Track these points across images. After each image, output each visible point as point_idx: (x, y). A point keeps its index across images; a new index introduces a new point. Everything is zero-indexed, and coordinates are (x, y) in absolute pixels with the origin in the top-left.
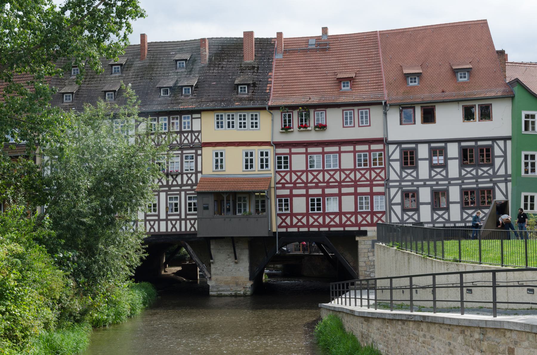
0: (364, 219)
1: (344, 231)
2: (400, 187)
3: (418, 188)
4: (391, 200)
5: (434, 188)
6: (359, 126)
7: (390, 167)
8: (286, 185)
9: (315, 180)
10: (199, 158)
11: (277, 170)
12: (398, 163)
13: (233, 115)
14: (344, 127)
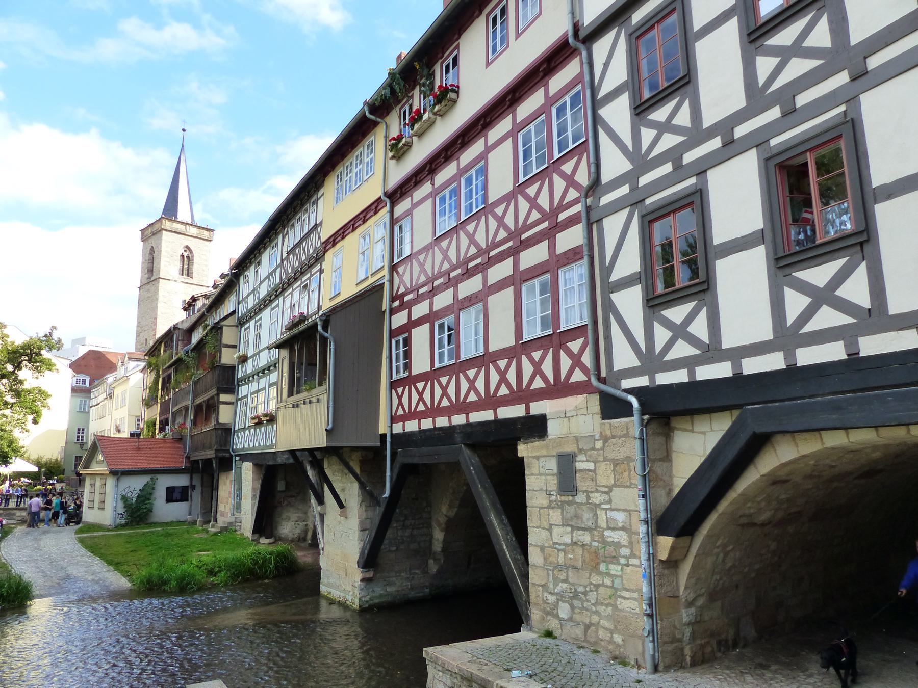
0: (538, 370)
1: (497, 422)
2: (634, 202)
3: (702, 173)
4: (607, 270)
5: (774, 142)
6: (518, 35)
7: (601, 132)
8: (406, 298)
9: (446, 266)
10: (322, 275)
11: (396, 261)
12: (624, 101)
13: (351, 163)
14: (488, 64)
